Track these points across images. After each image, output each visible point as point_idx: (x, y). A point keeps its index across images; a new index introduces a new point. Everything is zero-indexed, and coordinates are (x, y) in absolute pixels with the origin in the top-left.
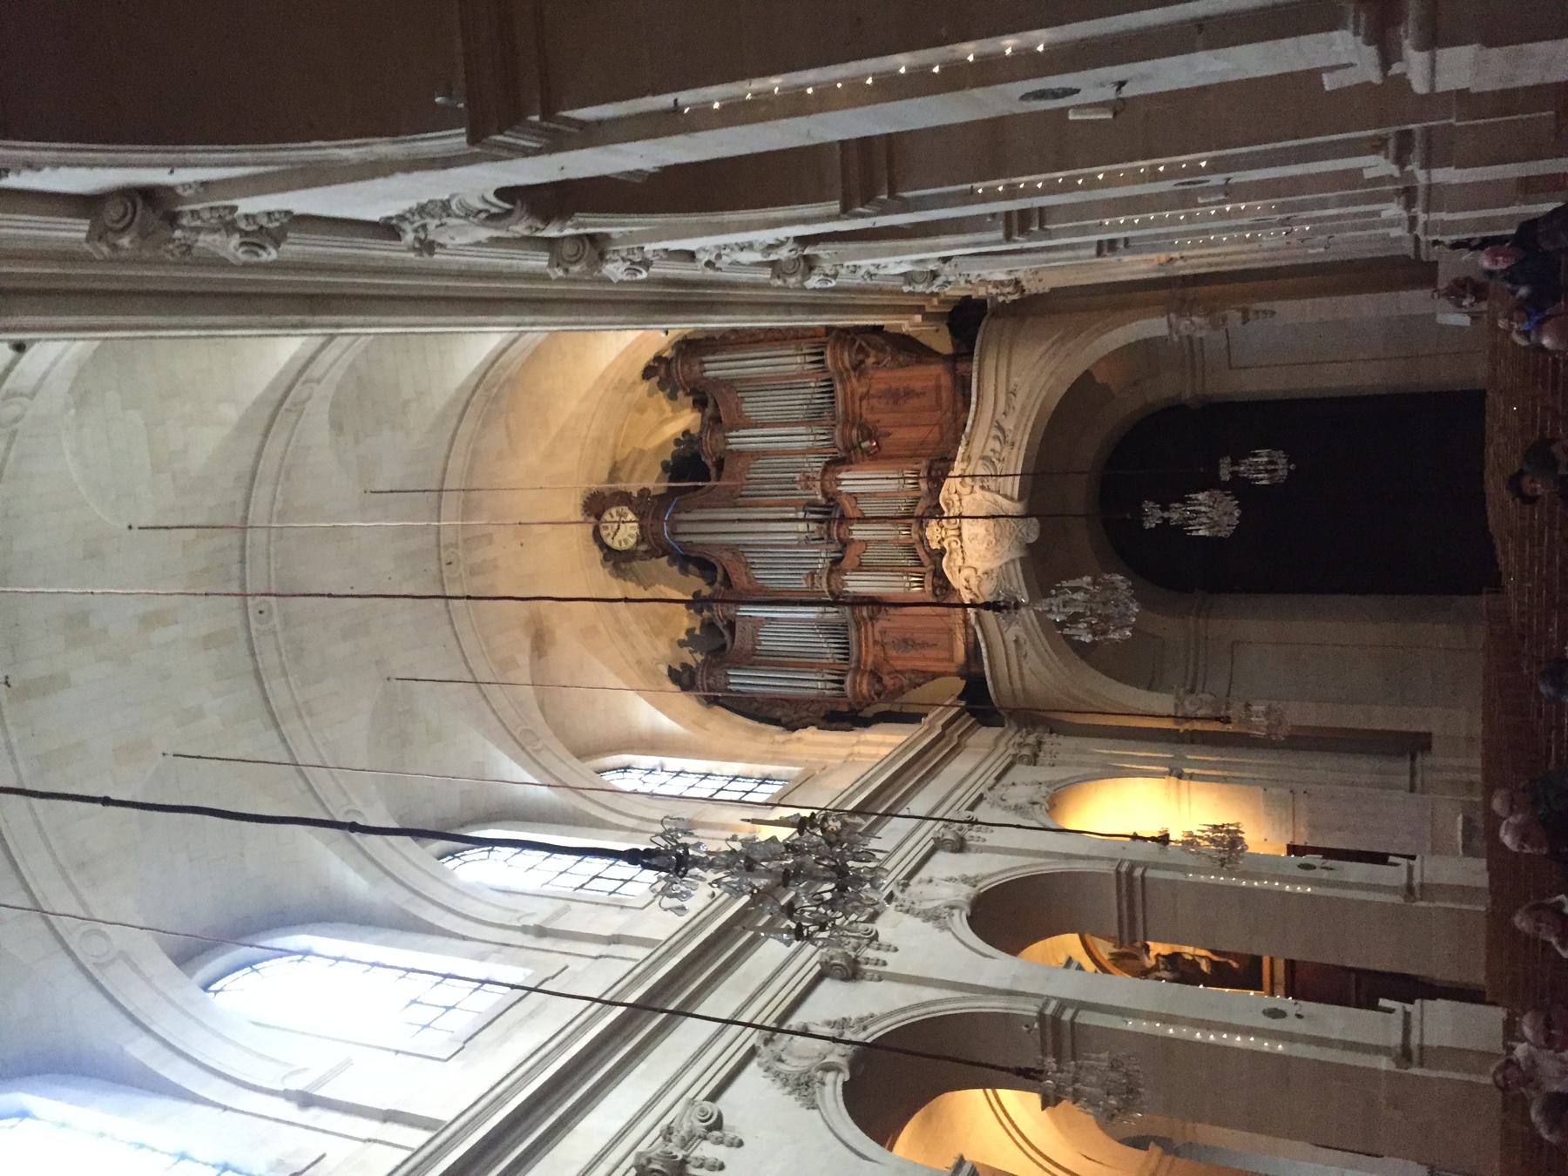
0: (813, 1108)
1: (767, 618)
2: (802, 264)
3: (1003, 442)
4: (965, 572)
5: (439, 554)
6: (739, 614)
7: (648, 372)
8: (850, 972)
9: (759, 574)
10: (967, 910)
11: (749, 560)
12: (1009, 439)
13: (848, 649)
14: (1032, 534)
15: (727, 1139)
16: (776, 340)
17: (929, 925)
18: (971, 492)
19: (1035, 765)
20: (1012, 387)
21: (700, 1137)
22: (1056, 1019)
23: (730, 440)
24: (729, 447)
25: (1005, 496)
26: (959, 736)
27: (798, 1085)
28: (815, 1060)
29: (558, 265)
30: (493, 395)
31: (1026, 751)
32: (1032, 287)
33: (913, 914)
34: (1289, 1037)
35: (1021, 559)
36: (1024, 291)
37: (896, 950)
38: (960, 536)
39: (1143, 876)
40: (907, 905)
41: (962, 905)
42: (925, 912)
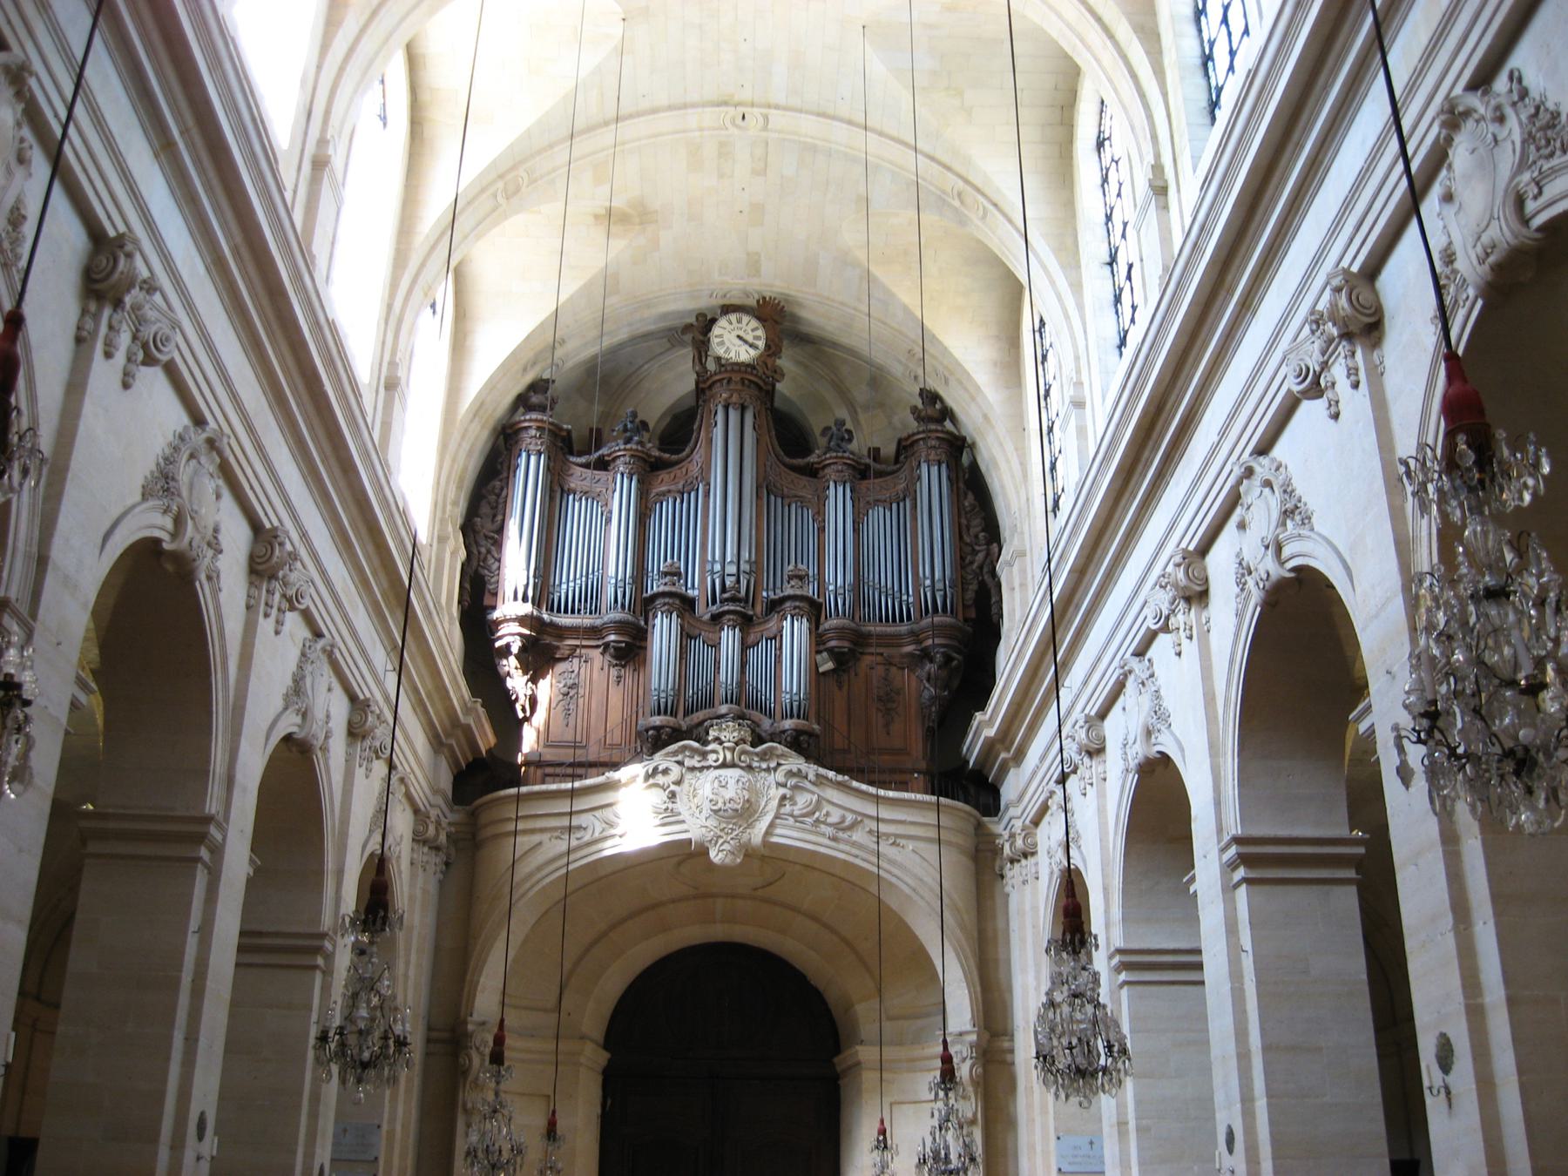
0: (143, 495)
1: (611, 512)
2: (1199, 589)
3: (838, 826)
4: (676, 771)
5: (760, 106)
6: (619, 476)
7: (931, 397)
8: (260, 568)
9: (667, 507)
10: (300, 735)
11: (685, 496)
12: (840, 834)
13: (566, 611)
14: (721, 855)
15: (132, 367)
16: (962, 559)
17: (290, 682)
18: (779, 785)
19: (413, 840)
20: (902, 842)
21: (137, 330)
22: (201, 838)
23: (840, 489)
24: (832, 485)
25: (772, 825)
26: (451, 747)
27: (167, 478)
28: (188, 506)
29: (1347, 281)
30: (950, 200)
31: (431, 830)
32: (1014, 874)
33: (301, 661)
34: (178, 1145)
35: (690, 841)
36: (1012, 861)
37: (277, 633)
38: (724, 765)
39: (315, 967)
40: (312, 657)
41: (306, 730)
42: (303, 677)
